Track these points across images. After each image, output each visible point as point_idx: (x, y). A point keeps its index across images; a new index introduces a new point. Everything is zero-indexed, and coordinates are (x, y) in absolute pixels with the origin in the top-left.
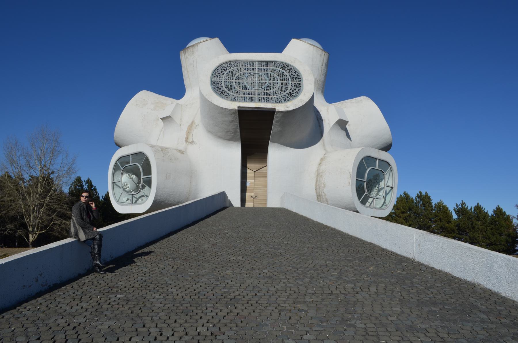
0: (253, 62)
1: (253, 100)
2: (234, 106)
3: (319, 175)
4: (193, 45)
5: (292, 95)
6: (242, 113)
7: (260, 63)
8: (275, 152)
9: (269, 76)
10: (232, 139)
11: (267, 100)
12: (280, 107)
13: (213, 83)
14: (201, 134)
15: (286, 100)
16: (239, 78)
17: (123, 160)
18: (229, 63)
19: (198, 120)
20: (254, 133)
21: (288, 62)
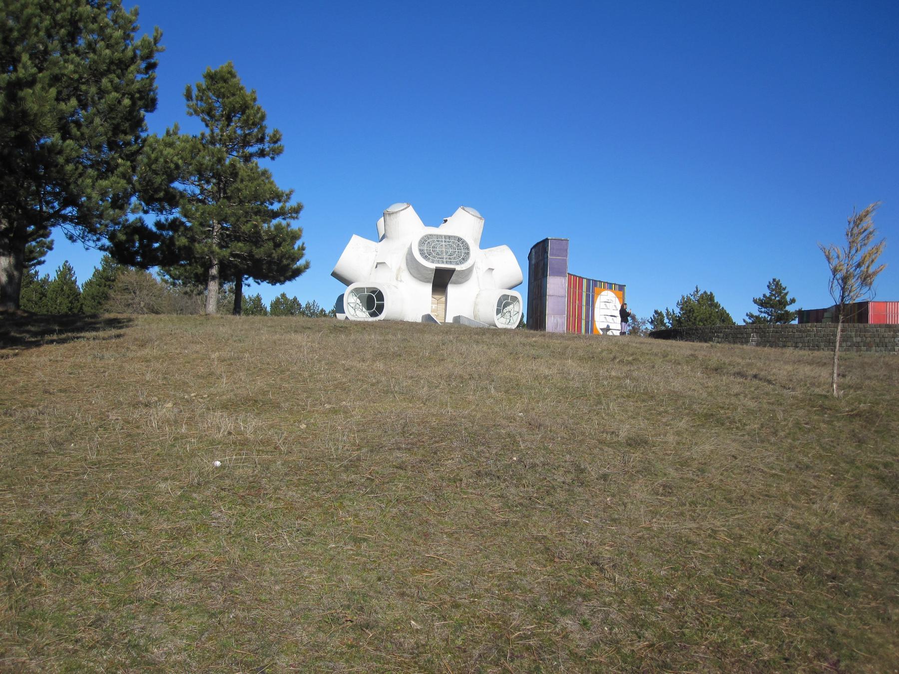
0: (441, 236)
1: (443, 262)
2: (433, 266)
3: (476, 304)
4: (396, 212)
5: (464, 260)
6: (438, 271)
7: (445, 237)
8: (451, 289)
9: (451, 246)
10: (428, 282)
11: (451, 263)
12: (458, 268)
13: (420, 250)
14: (406, 276)
15: (461, 263)
16: (434, 247)
17: (357, 291)
18: (429, 237)
19: (404, 266)
20: (441, 281)
21: (461, 236)
